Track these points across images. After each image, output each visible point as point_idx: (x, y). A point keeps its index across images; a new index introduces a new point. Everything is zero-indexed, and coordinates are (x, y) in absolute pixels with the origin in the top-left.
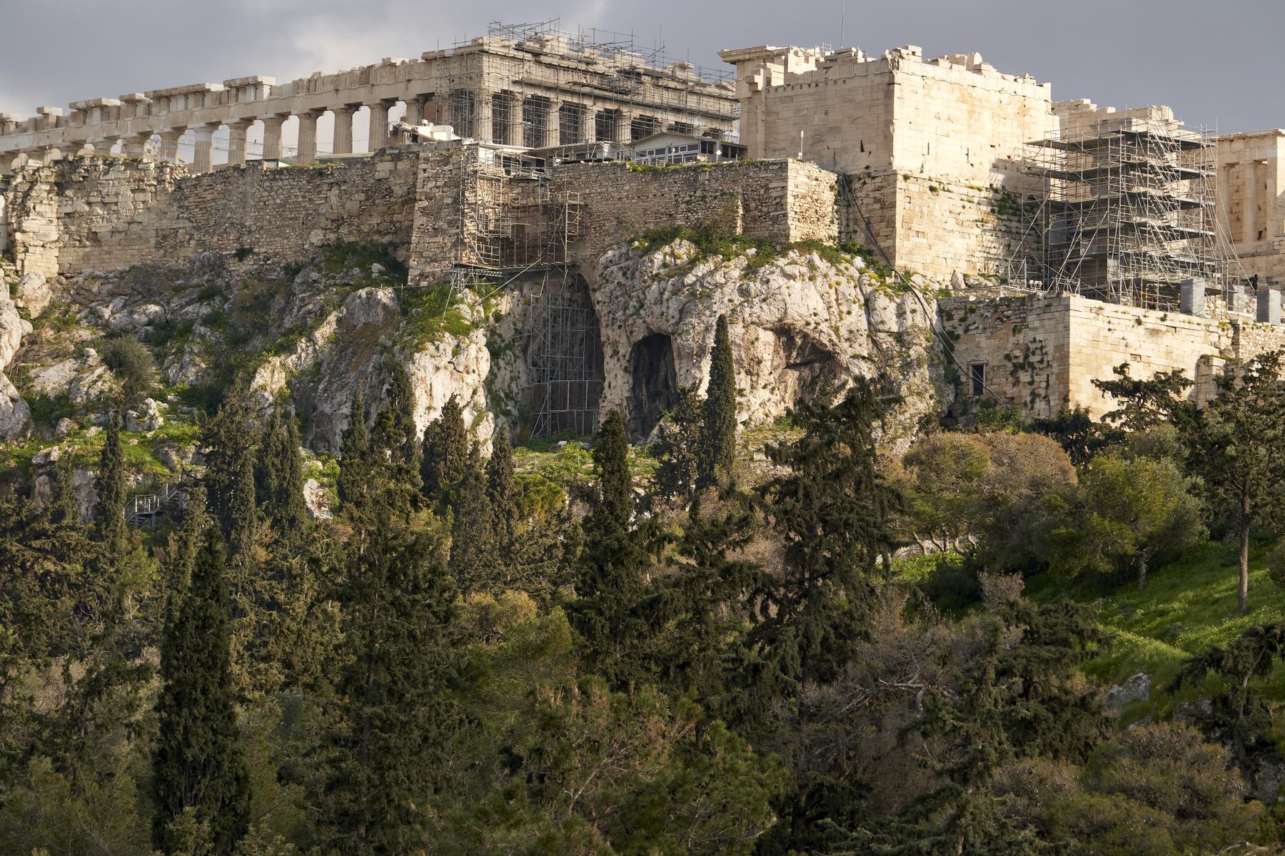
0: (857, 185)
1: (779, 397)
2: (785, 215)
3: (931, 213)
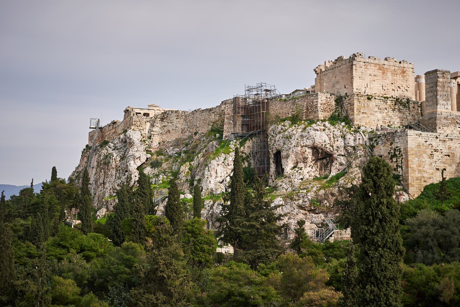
0: (344, 99)
1: (315, 170)
3: (368, 106)
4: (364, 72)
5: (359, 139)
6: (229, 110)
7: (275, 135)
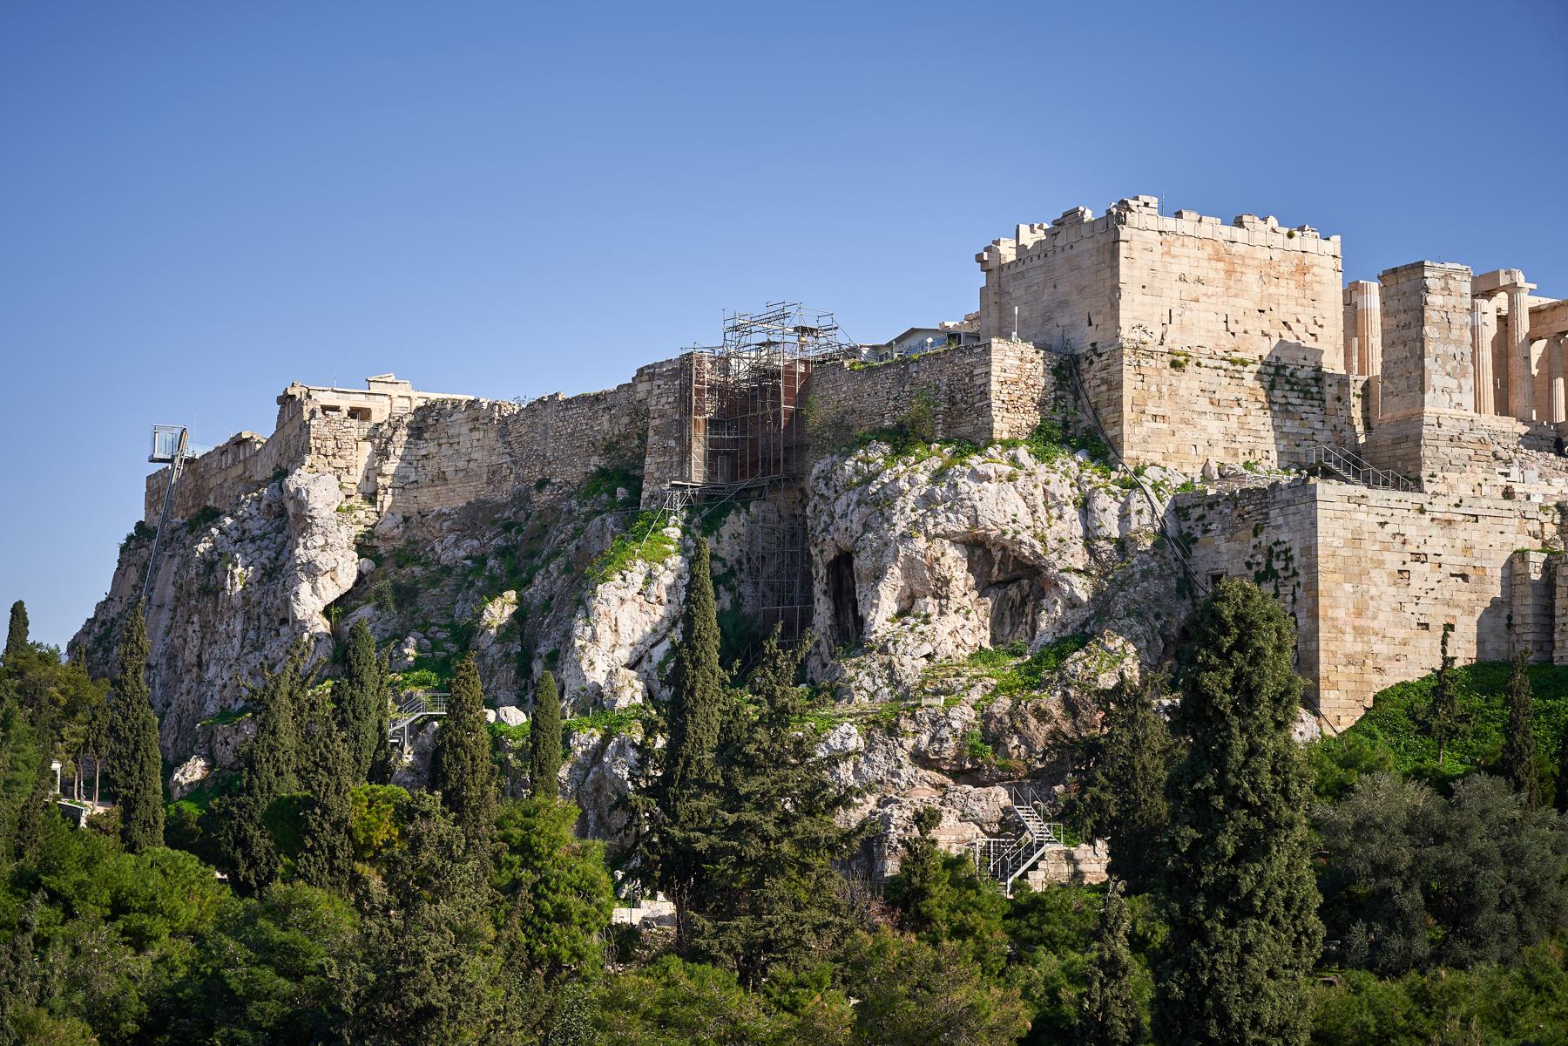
0: (1084, 365)
2: (989, 405)
3: (1173, 393)
4: (1158, 266)
5: (1140, 512)
6: (663, 400)
7: (832, 495)
